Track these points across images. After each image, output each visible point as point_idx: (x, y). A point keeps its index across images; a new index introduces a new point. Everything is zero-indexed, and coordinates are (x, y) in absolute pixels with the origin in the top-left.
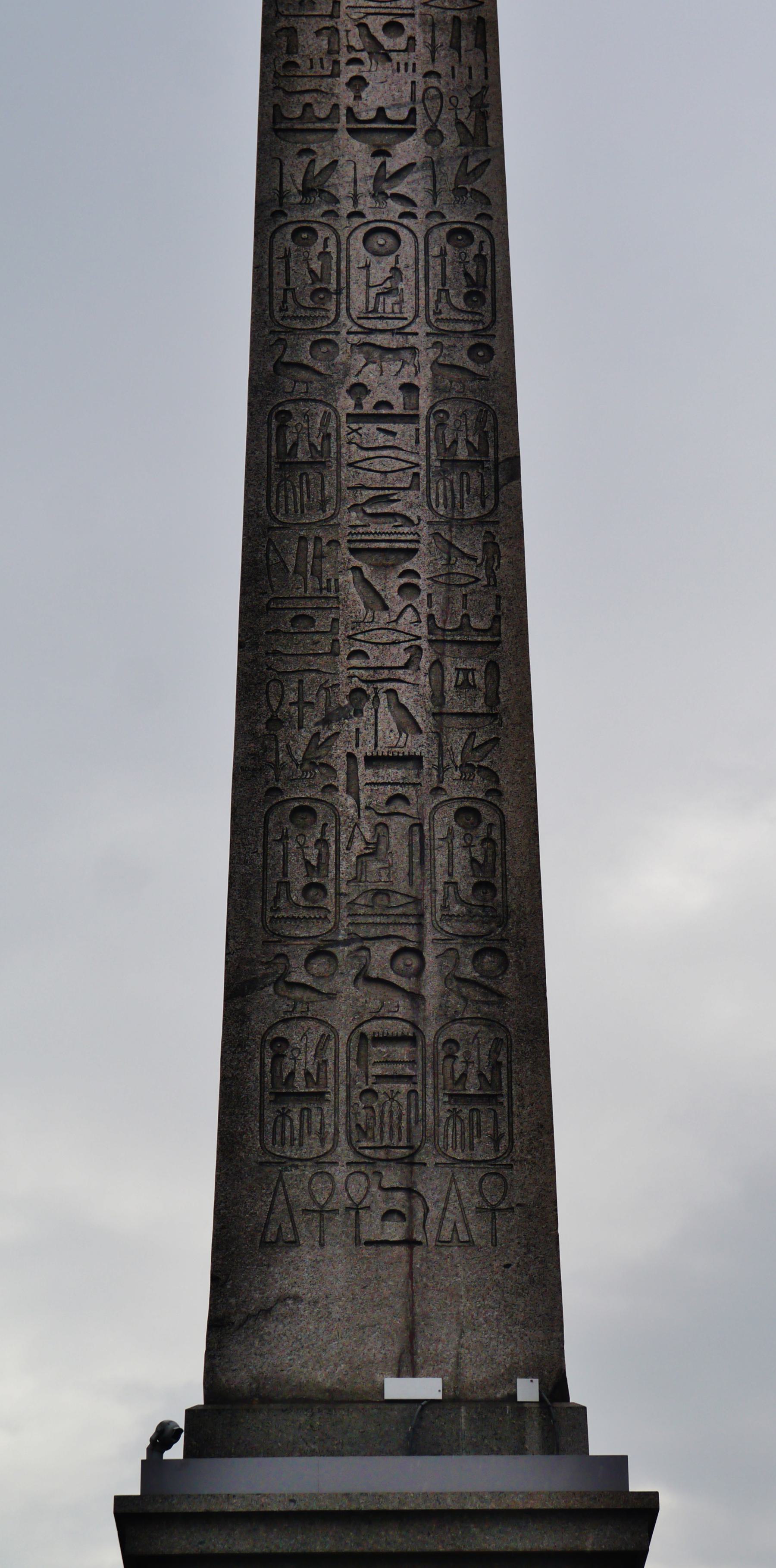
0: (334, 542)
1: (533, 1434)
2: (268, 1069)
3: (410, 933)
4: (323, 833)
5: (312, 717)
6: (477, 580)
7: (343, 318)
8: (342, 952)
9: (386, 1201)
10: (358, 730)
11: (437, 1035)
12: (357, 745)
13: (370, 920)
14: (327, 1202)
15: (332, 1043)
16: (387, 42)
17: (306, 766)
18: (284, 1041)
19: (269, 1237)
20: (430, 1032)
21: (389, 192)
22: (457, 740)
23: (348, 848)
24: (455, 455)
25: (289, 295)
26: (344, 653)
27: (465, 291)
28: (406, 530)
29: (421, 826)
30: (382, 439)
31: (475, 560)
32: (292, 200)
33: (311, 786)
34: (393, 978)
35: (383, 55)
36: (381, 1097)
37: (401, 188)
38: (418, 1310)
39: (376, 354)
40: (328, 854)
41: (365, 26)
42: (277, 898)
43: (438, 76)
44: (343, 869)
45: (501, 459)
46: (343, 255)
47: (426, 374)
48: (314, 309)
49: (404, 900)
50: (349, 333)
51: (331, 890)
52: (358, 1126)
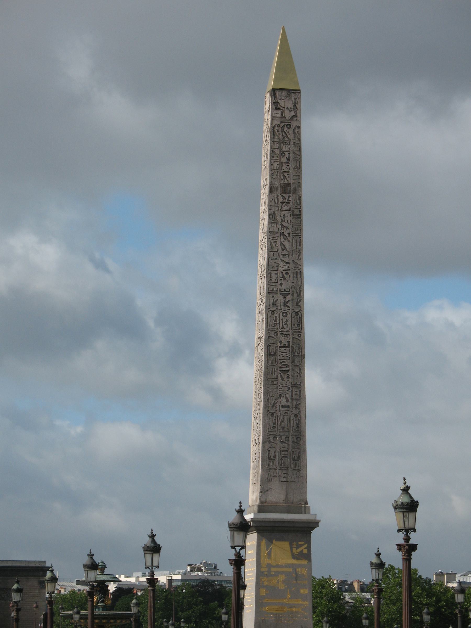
0: (277, 369)
4: (275, 418)
5: (274, 398)
6: (298, 376)
7: (279, 329)
8: (278, 437)
9: (284, 475)
11: (291, 450)
13: (282, 432)
15: (276, 451)
16: (286, 276)
20: (290, 450)
21: (286, 305)
22: (295, 403)
25: (270, 324)
26: (278, 389)
27: (297, 324)
28: (288, 367)
30: (284, 351)
31: (298, 372)
32: (271, 306)
33: (274, 410)
34: (285, 441)
35: (285, 278)
44: (278, 424)
45: (302, 355)
46: (279, 317)
47: (291, 339)
49: (287, 429)
50: (280, 331)
52: (280, 464)
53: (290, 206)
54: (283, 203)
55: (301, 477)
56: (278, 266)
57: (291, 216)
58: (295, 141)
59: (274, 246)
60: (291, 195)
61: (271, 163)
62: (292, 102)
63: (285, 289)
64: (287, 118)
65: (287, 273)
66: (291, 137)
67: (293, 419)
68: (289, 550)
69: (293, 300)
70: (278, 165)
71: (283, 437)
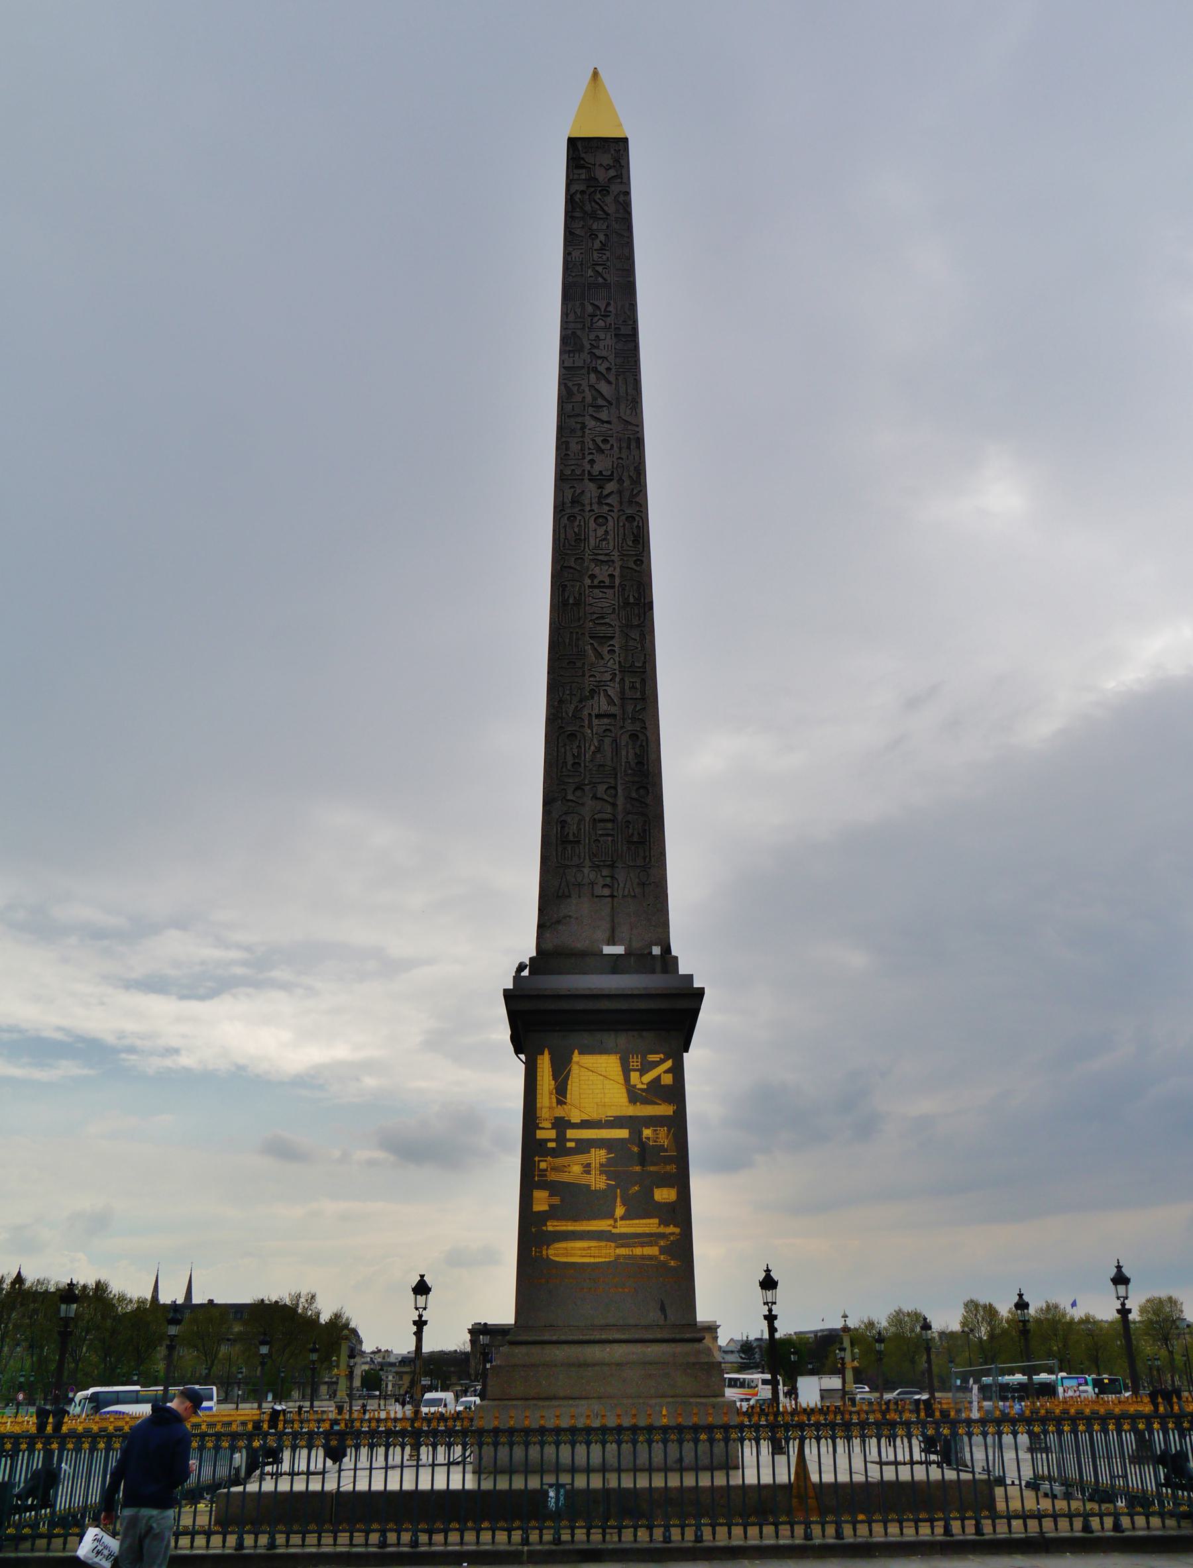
1: (658, 967)
2: (559, 832)
3: (612, 781)
4: (579, 743)
6: (637, 648)
7: (587, 549)
10: (592, 705)
11: (622, 819)
12: (592, 710)
14: (582, 881)
16: (603, 446)
17: (573, 718)
18: (565, 821)
19: (560, 895)
20: (620, 818)
21: (604, 502)
22: (630, 709)
23: (589, 749)
24: (629, 601)
25: (566, 541)
27: (632, 539)
28: (610, 629)
29: (616, 741)
30: (601, 595)
34: (605, 797)
35: (602, 451)
36: (602, 842)
37: (608, 501)
38: (615, 921)
39: (599, 563)
40: (581, 752)
41: (595, 440)
42: (562, 768)
43: (622, 459)
44: (587, 757)
46: (587, 525)
47: (618, 569)
48: (575, 546)
49: (610, 768)
50: (589, 555)
51: (583, 765)
52: (593, 853)
53: (608, 320)
54: (592, 316)
55: (651, 884)
56: (583, 426)
57: (613, 337)
58: (617, 215)
59: (576, 392)
60: (612, 302)
61: (567, 252)
62: (610, 156)
63: (601, 472)
64: (601, 179)
65: (605, 441)
66: (611, 209)
67: (627, 745)
68: (621, 1079)
69: (620, 492)
70: (581, 253)
71: (601, 789)
